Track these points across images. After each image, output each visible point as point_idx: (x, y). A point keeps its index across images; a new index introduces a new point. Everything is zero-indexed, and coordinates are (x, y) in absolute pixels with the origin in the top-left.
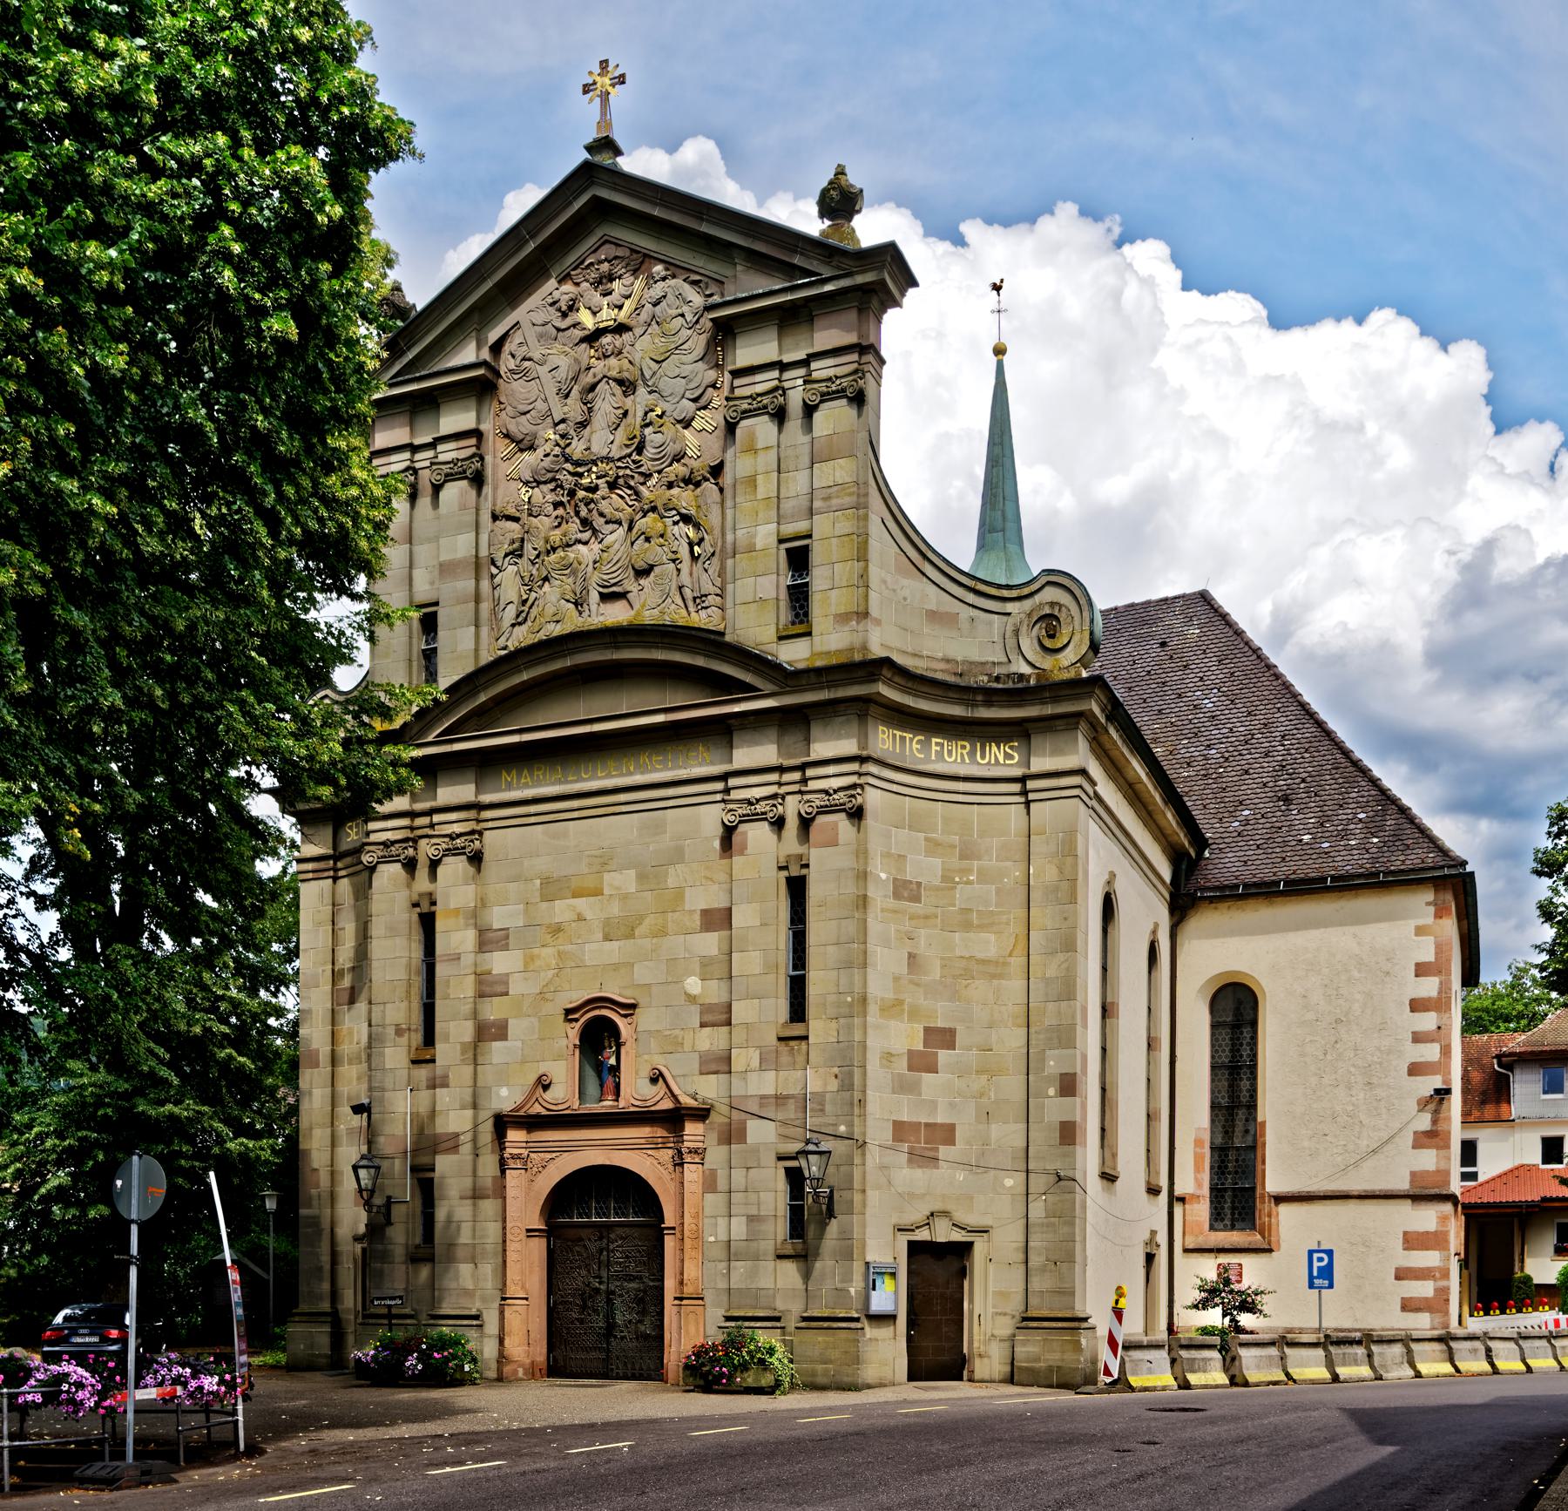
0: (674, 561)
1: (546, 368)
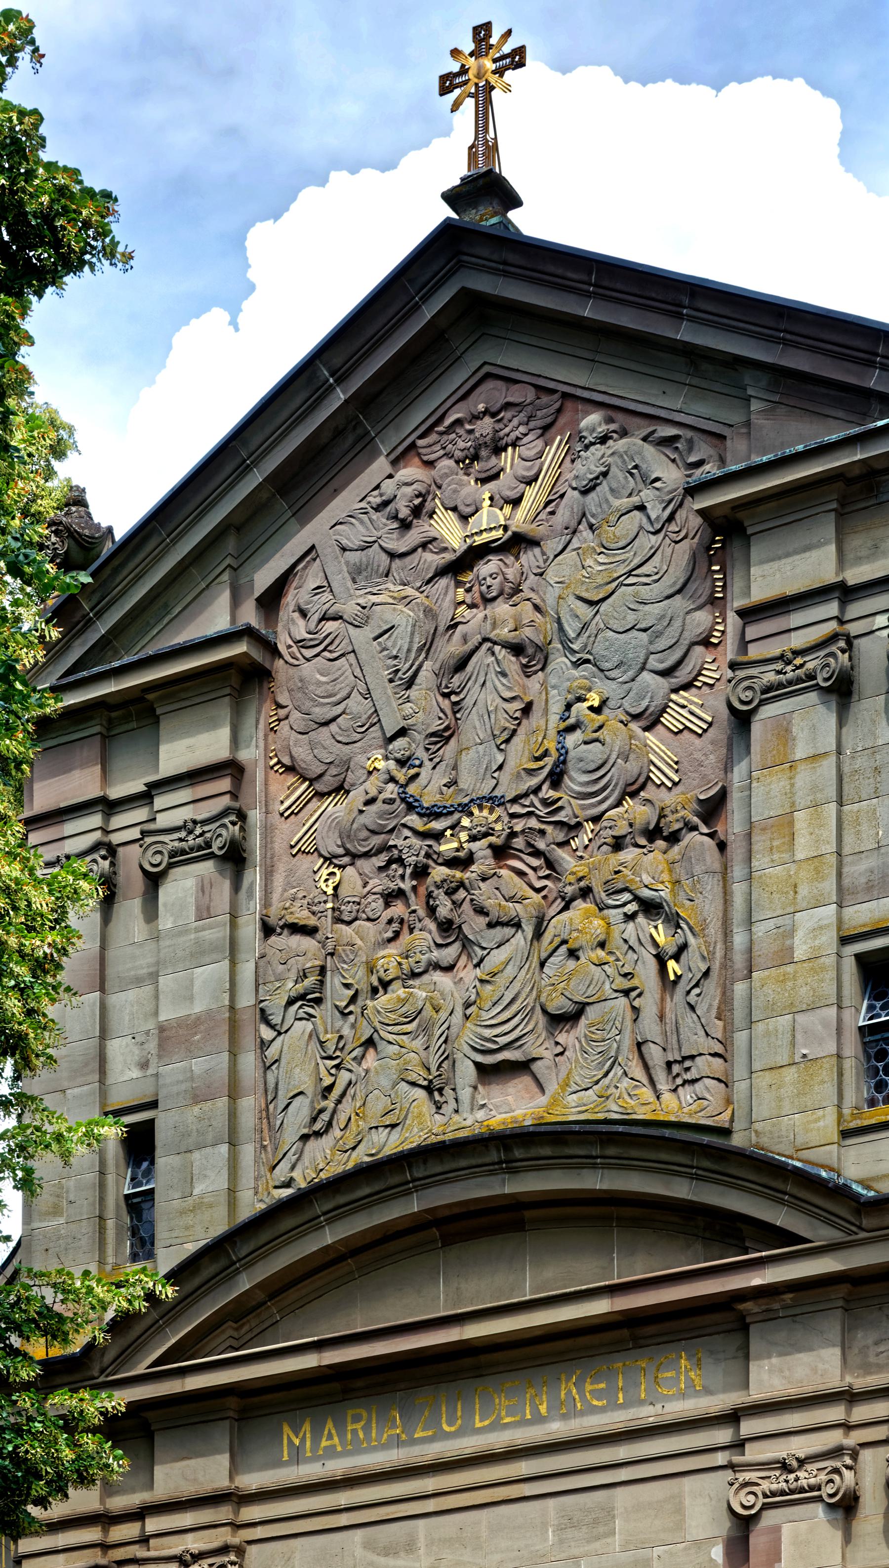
0: (626, 993)
1: (369, 632)
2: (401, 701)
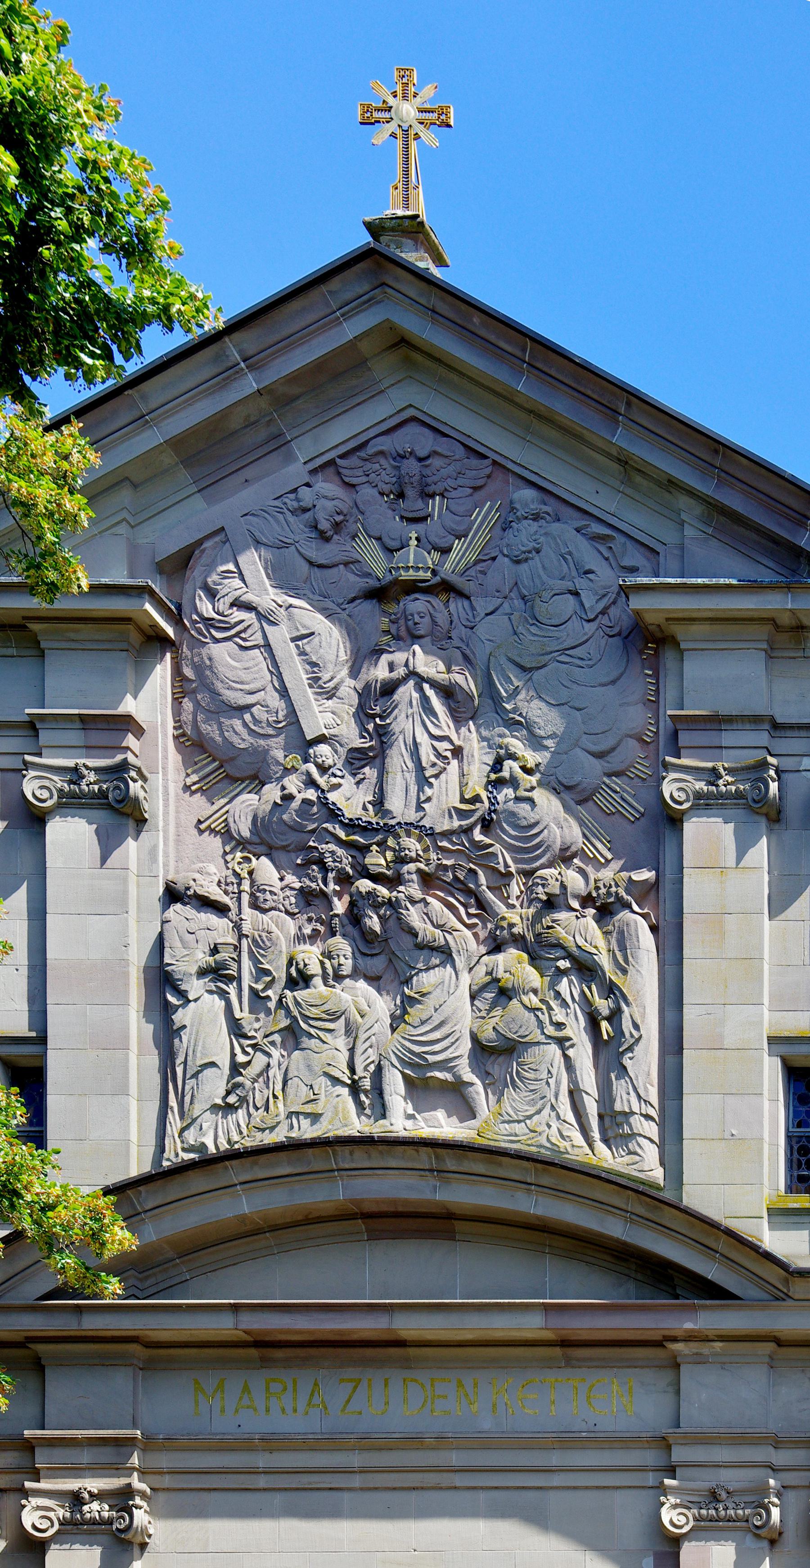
2: (321, 709)
